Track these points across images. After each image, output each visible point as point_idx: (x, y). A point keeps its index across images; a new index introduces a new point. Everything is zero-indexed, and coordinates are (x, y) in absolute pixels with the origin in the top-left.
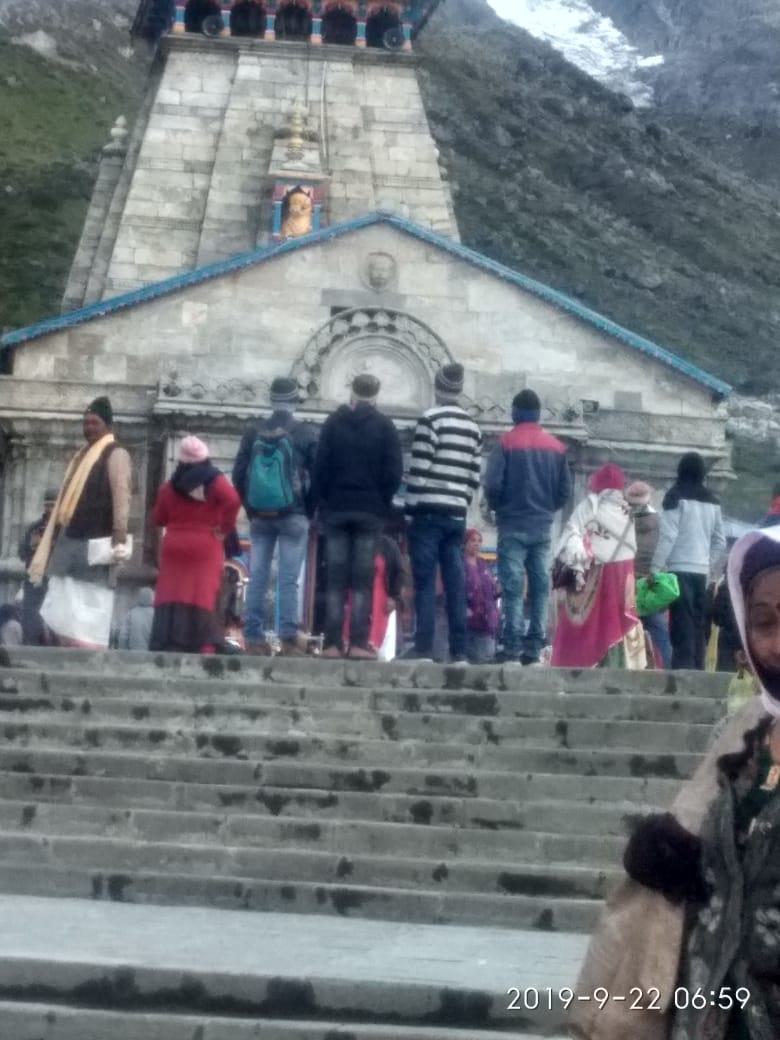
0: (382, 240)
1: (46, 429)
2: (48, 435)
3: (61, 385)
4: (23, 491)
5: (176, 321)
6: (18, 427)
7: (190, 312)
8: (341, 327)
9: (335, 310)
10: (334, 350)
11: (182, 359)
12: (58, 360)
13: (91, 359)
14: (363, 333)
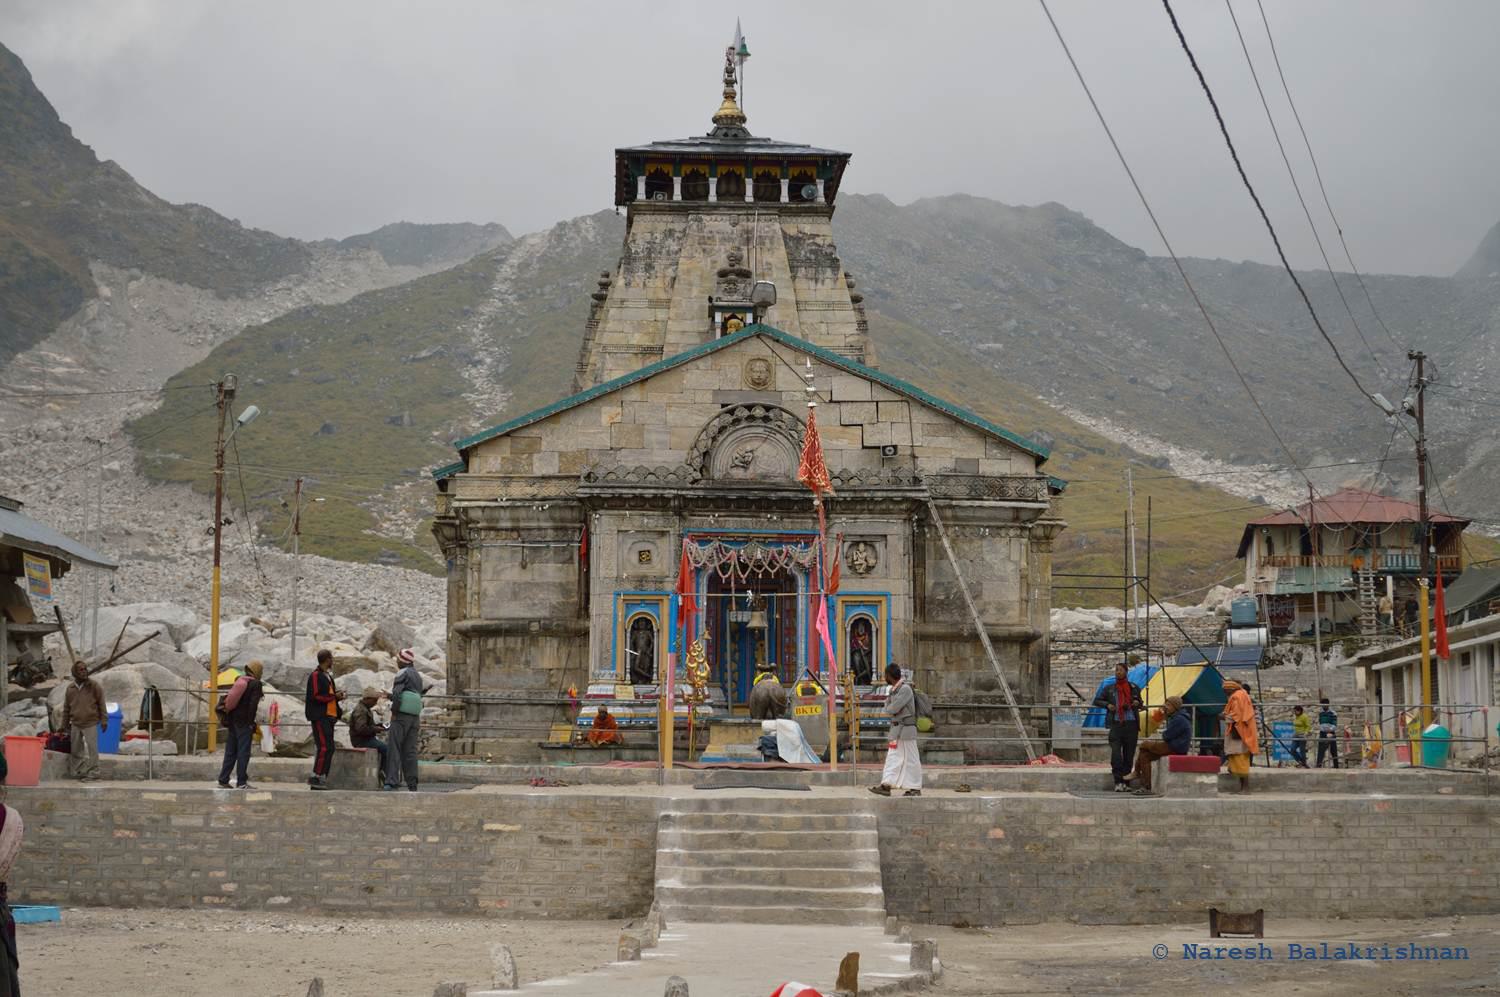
0: (758, 348)
2: (498, 521)
6: (473, 514)
7: (608, 413)
8: (729, 418)
10: (721, 438)
11: (602, 452)
12: (503, 458)
13: (531, 454)
14: (744, 424)
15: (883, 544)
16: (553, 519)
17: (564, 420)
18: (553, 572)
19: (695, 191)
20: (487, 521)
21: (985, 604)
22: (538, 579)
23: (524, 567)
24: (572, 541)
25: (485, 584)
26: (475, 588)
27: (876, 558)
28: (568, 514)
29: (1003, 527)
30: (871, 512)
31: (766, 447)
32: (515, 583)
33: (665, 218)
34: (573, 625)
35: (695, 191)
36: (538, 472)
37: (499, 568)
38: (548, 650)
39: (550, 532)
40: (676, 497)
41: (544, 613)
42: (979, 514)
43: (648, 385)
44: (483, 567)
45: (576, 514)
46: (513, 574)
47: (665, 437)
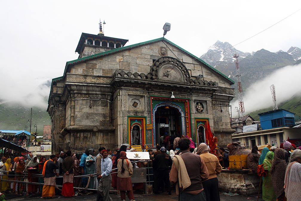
0: (162, 44)
1: (81, 88)
2: (81, 90)
3: (85, 76)
4: (75, 106)
5: (115, 61)
6: (73, 88)
9: (154, 61)
10: (160, 67)
12: (83, 70)
13: (93, 69)
14: (166, 63)
15: (205, 103)
16: (101, 91)
17: (104, 59)
18: (100, 109)
19: (97, 43)
20: (77, 90)
21: (223, 123)
22: (95, 112)
23: (91, 108)
24: (107, 99)
25: (76, 113)
26: (72, 115)
27: (203, 107)
28: (107, 90)
29: (225, 102)
30: (202, 93)
31: (173, 71)
32: (87, 113)
33: (91, 48)
34: (110, 128)
35: (97, 43)
36: (95, 75)
37: (82, 107)
38: (99, 137)
39: (100, 96)
40: (149, 84)
41: (98, 124)
42: (221, 97)
43: (132, 51)
44: (76, 107)
45: (109, 90)
46: (86, 110)
47: (137, 68)
